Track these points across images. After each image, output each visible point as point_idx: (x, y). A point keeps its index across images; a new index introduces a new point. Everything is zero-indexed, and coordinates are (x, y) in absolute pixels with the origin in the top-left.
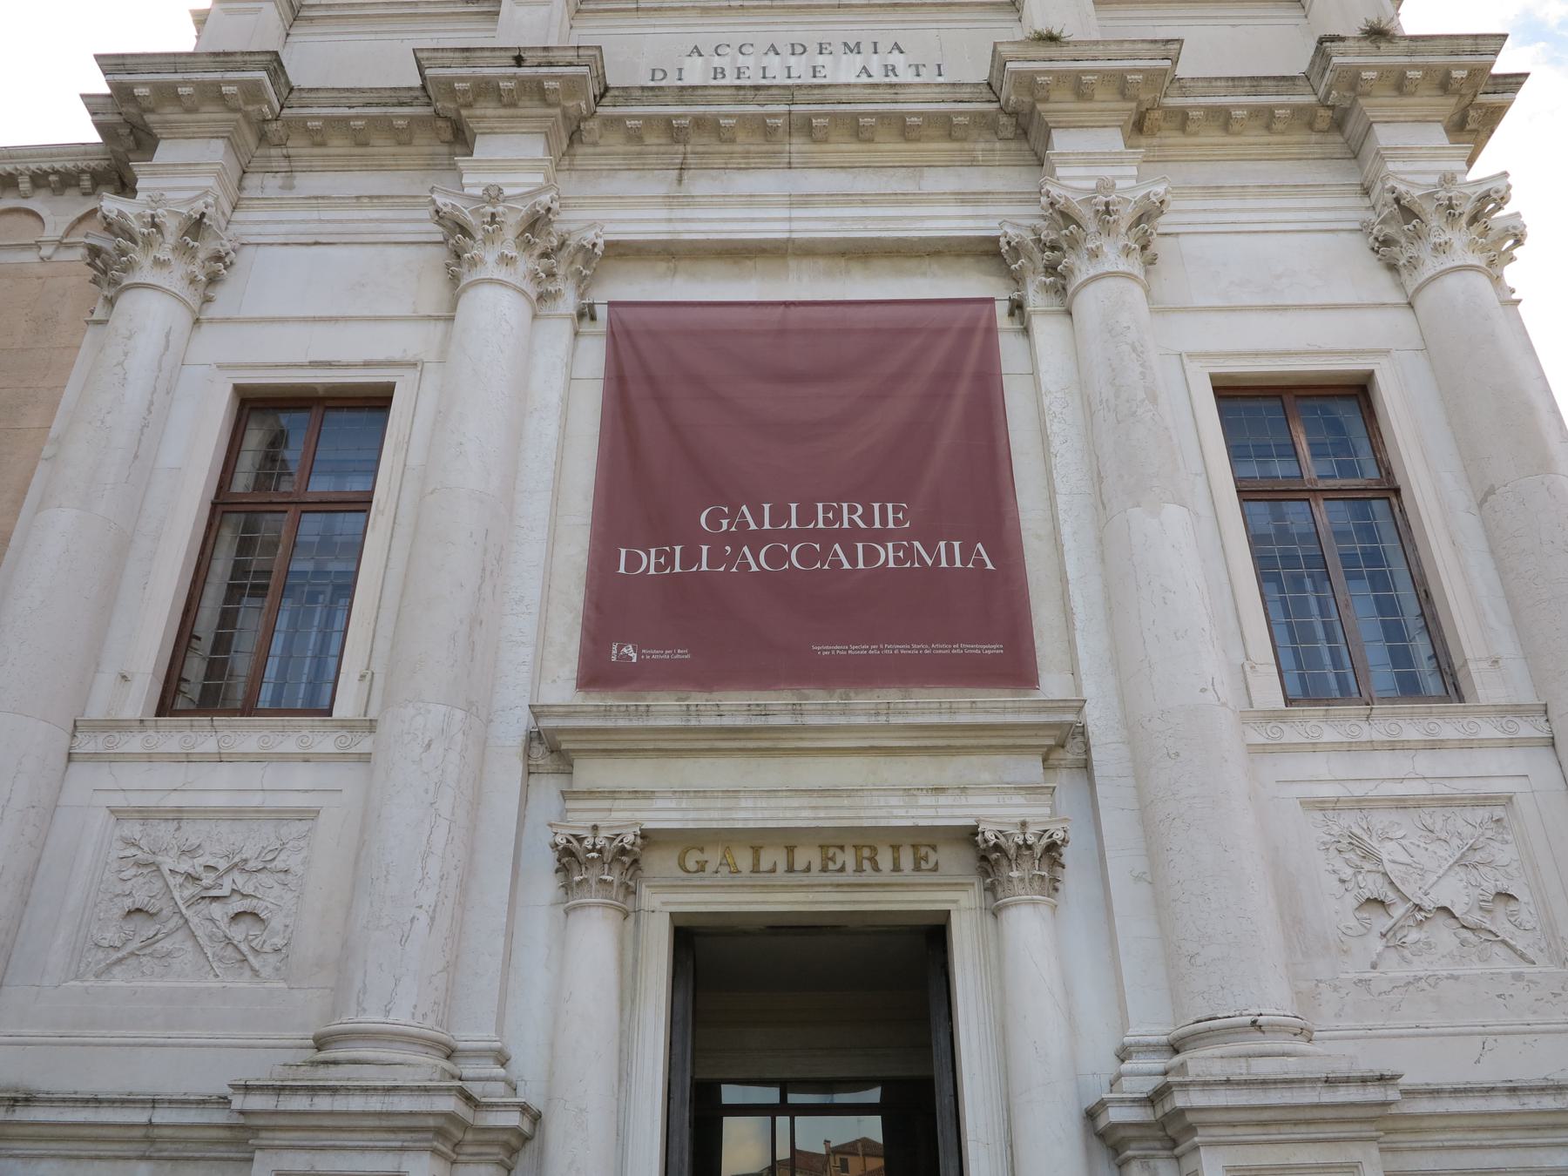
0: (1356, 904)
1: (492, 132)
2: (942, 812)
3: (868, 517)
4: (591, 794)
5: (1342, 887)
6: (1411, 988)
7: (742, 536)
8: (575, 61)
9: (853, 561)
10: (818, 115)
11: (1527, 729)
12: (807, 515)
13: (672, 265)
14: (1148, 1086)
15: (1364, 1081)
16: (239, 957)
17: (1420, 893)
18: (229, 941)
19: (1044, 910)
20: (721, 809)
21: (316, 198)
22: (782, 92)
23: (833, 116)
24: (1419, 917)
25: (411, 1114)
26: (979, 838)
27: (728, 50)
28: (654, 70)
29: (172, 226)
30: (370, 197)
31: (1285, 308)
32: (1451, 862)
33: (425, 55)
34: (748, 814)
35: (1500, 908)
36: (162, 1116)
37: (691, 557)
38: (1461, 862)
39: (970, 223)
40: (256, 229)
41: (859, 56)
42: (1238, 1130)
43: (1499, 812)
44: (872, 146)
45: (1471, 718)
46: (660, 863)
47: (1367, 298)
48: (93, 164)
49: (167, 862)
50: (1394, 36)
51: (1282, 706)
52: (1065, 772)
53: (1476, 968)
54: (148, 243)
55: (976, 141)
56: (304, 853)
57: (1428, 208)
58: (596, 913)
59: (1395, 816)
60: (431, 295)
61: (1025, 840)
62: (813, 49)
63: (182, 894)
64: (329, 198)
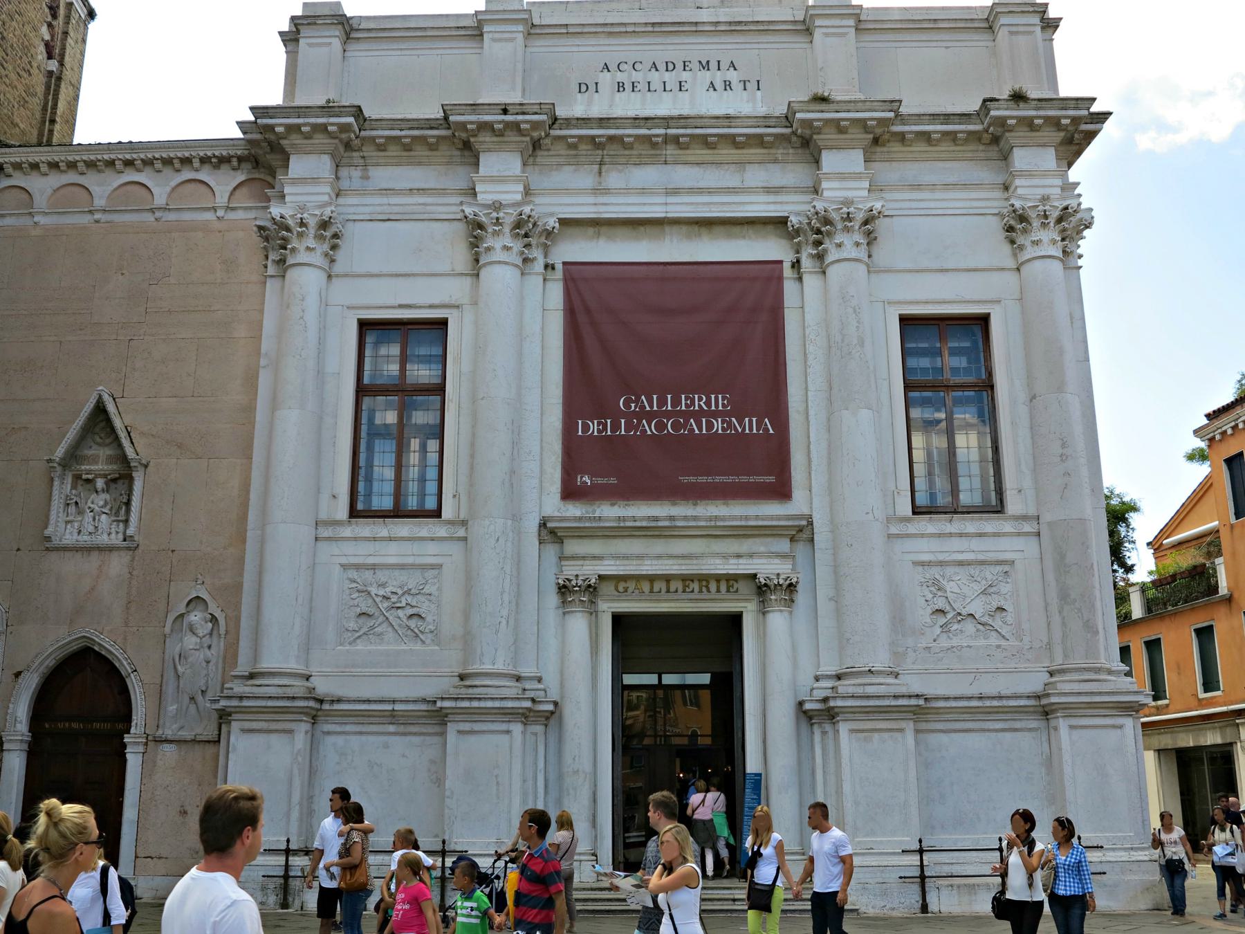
1: (489, 150)
2: (741, 567)
3: (708, 403)
4: (573, 558)
6: (949, 651)
7: (643, 414)
8: (539, 111)
9: (700, 429)
10: (683, 136)
11: (1027, 528)
13: (596, 229)
15: (910, 697)
18: (409, 628)
19: (786, 614)
20: (637, 565)
21: (386, 190)
22: (662, 121)
23: (691, 136)
24: (959, 619)
25: (513, 708)
26: (757, 580)
29: (312, 223)
30: (418, 190)
31: (947, 270)
32: (979, 592)
33: (449, 108)
34: (648, 568)
35: (998, 615)
36: (398, 707)
37: (616, 427)
39: (772, 207)
40: (352, 210)
42: (856, 715)
43: (1006, 568)
44: (716, 151)
45: (1001, 522)
46: (607, 589)
47: (996, 263)
48: (239, 153)
49: (373, 590)
50: (1028, 99)
52: (802, 543)
53: (982, 642)
54: (300, 235)
55: (778, 148)
56: (437, 585)
57: (1032, 214)
59: (957, 569)
60: (460, 257)
62: (680, 66)
64: (393, 190)
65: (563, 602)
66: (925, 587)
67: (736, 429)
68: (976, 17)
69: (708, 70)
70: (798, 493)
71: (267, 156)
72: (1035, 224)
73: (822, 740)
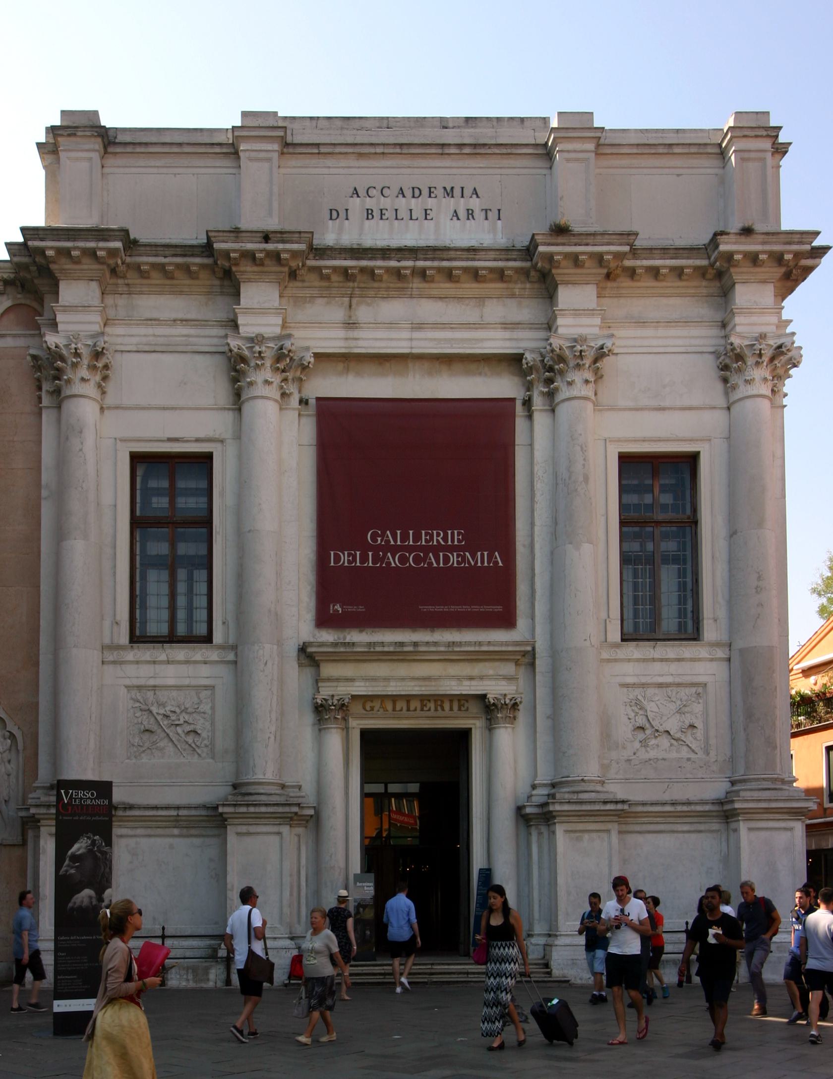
0: (633, 729)
2: (472, 688)
3: (445, 539)
5: (629, 721)
6: (647, 763)
7: (387, 548)
9: (438, 562)
12: (417, 537)
14: (543, 800)
16: (192, 749)
17: (659, 725)
18: (187, 743)
19: (509, 730)
21: (151, 320)
24: (656, 735)
26: (487, 700)
27: (375, 191)
28: (331, 210)
30: (182, 320)
34: (393, 688)
35: (690, 732)
37: (364, 559)
38: (679, 712)
41: (452, 199)
46: (356, 708)
49: (154, 709)
51: (620, 640)
56: (210, 705)
58: (334, 731)
59: (657, 691)
61: (505, 702)
63: (164, 723)
64: (158, 320)
65: (319, 720)
66: (628, 706)
67: (469, 563)
68: (708, 141)
69: (452, 197)
70: (522, 622)
71: (36, 281)
72: (749, 363)
73: (538, 839)
